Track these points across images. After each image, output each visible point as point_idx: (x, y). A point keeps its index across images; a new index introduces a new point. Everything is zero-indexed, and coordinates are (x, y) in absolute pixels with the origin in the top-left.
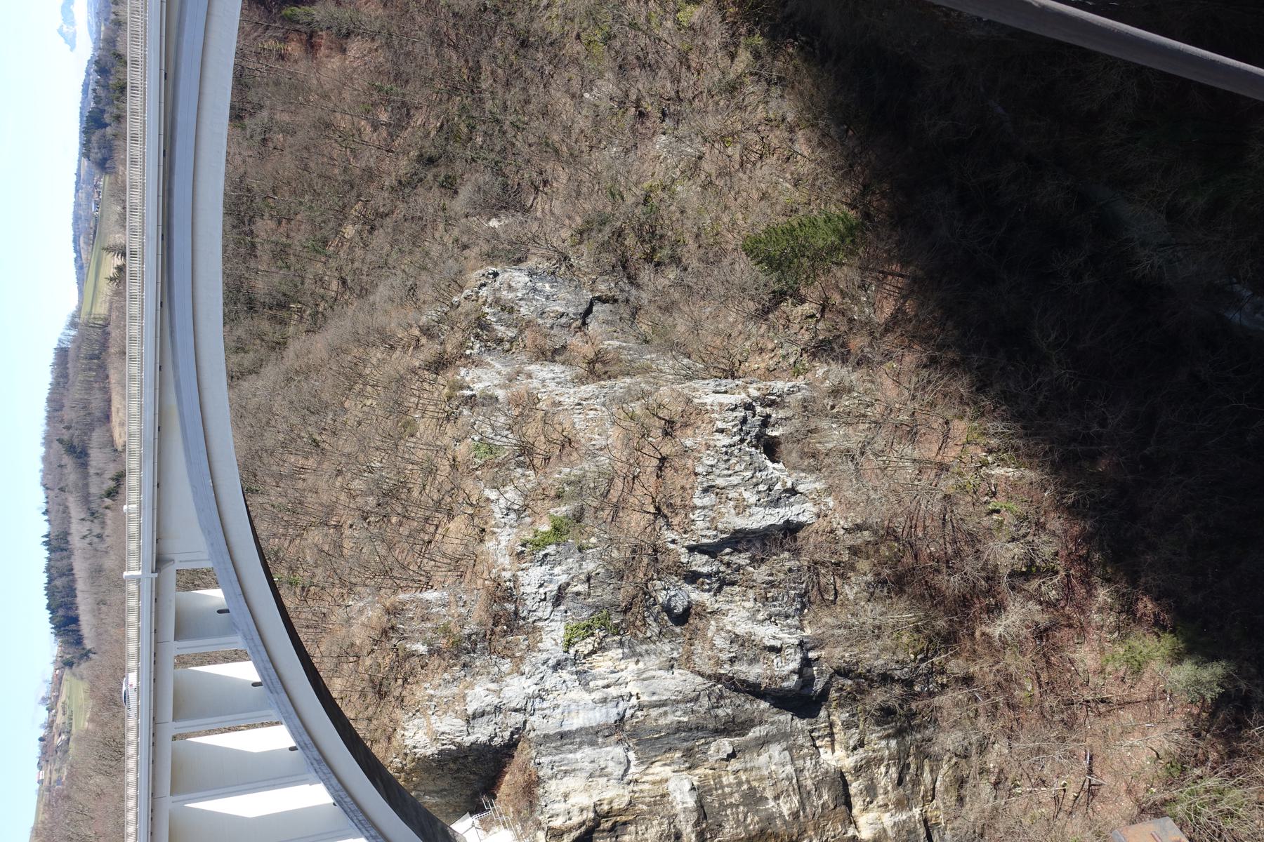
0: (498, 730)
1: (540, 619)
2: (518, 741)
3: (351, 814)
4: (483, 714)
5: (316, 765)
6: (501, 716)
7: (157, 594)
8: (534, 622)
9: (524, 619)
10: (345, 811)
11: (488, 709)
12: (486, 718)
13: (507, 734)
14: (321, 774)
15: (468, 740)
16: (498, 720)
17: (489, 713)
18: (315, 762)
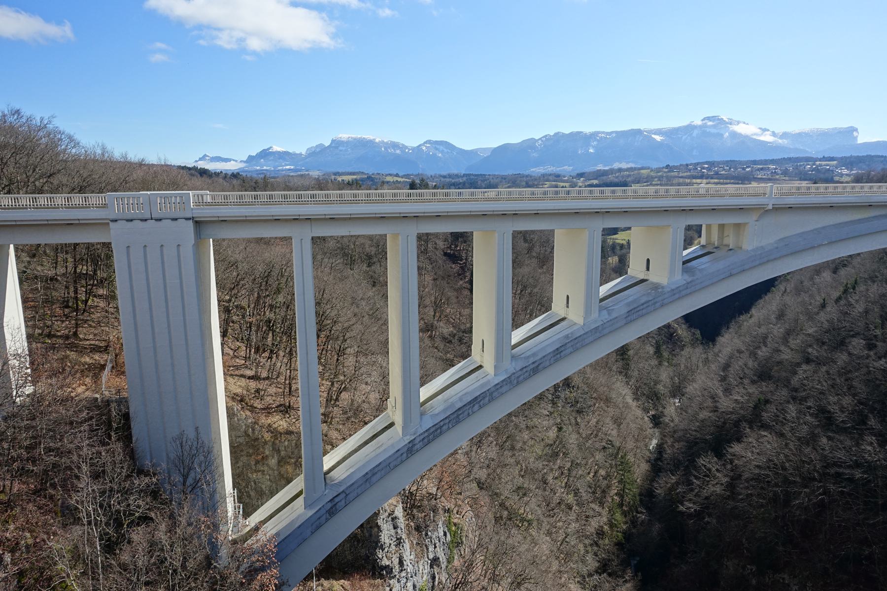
0: (386, 550)
1: (428, 549)
2: (381, 577)
3: (455, 415)
4: (395, 527)
5: (532, 367)
6: (394, 547)
7: (410, 217)
8: (426, 546)
9: (427, 534)
10: (459, 409)
11: (399, 531)
12: (393, 532)
13: (385, 562)
14: (520, 373)
15: (380, 522)
16: (392, 546)
17: (397, 533)
18: (536, 364)
